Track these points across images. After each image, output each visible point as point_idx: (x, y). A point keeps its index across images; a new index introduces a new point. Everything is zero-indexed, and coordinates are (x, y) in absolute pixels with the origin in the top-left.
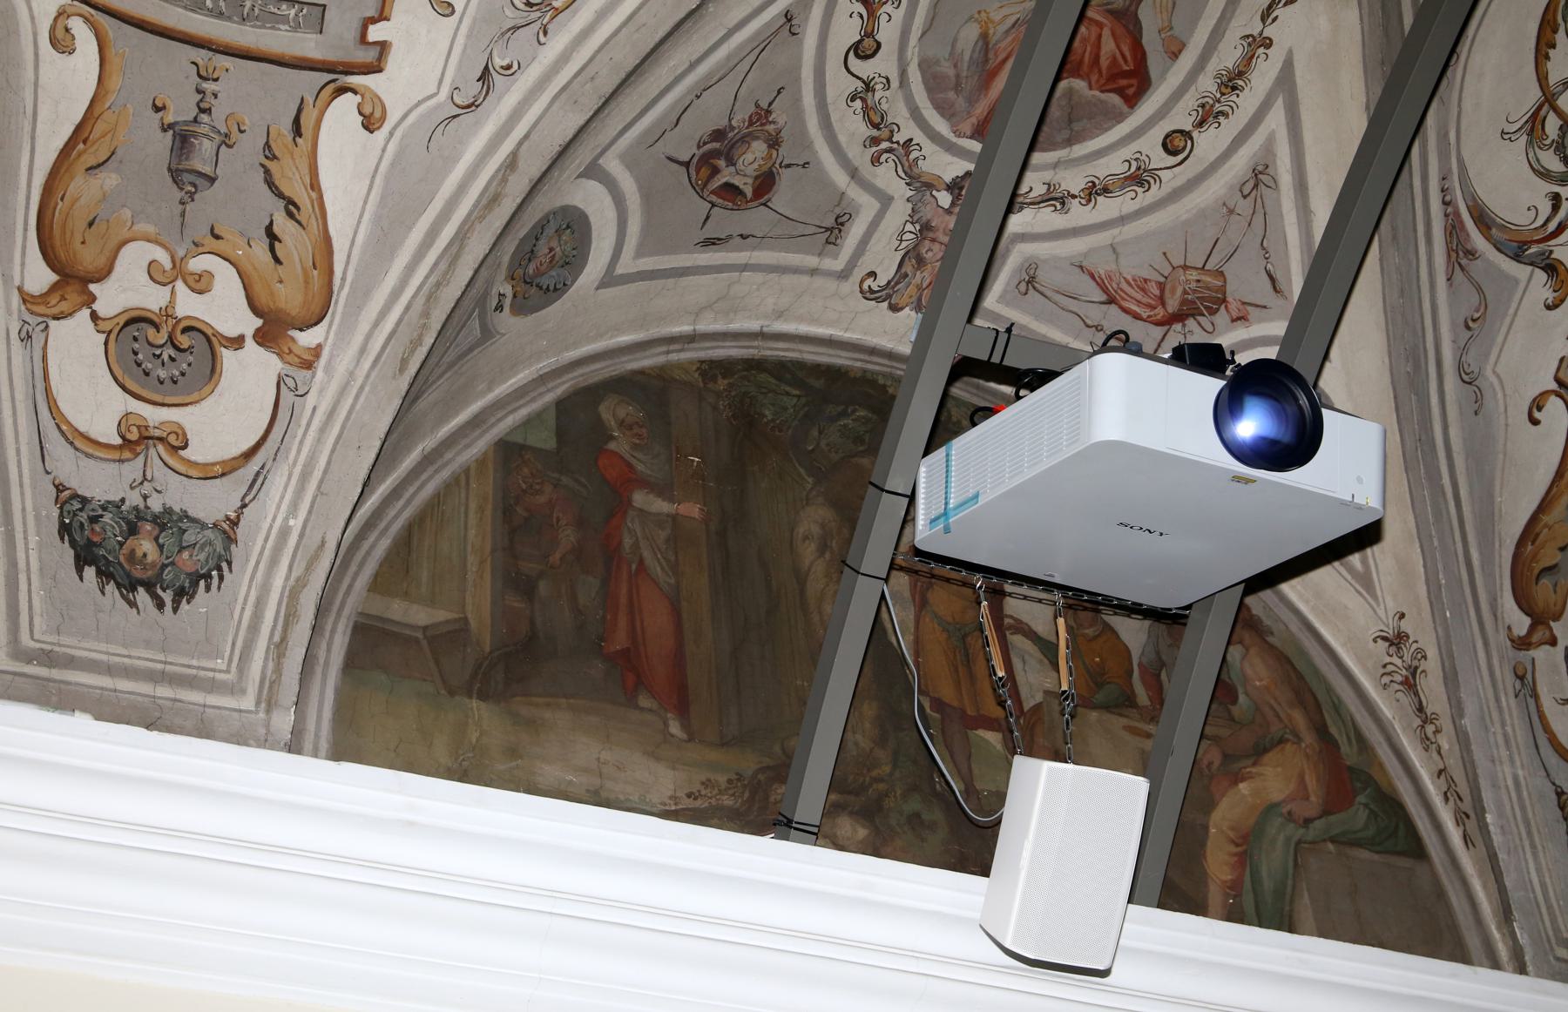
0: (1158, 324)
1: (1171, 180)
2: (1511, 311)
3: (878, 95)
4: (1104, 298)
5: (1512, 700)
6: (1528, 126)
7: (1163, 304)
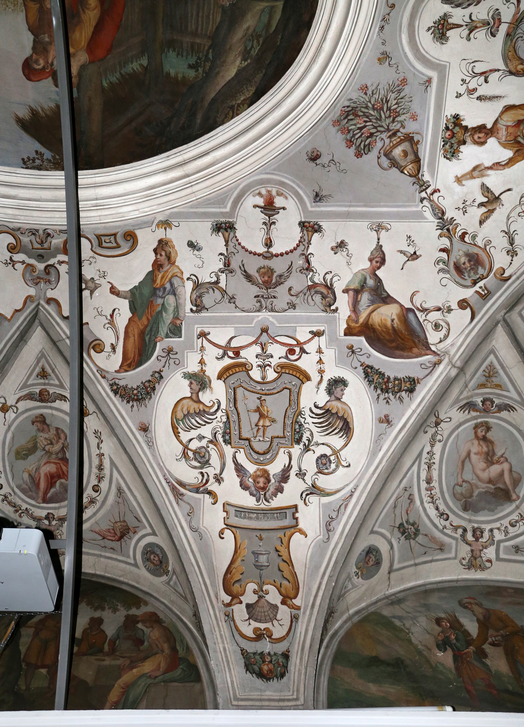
0: (118, 541)
1: (100, 499)
2: (202, 508)
3: (10, 498)
4: (102, 538)
5: (224, 623)
6: (183, 456)
7: (116, 534)
